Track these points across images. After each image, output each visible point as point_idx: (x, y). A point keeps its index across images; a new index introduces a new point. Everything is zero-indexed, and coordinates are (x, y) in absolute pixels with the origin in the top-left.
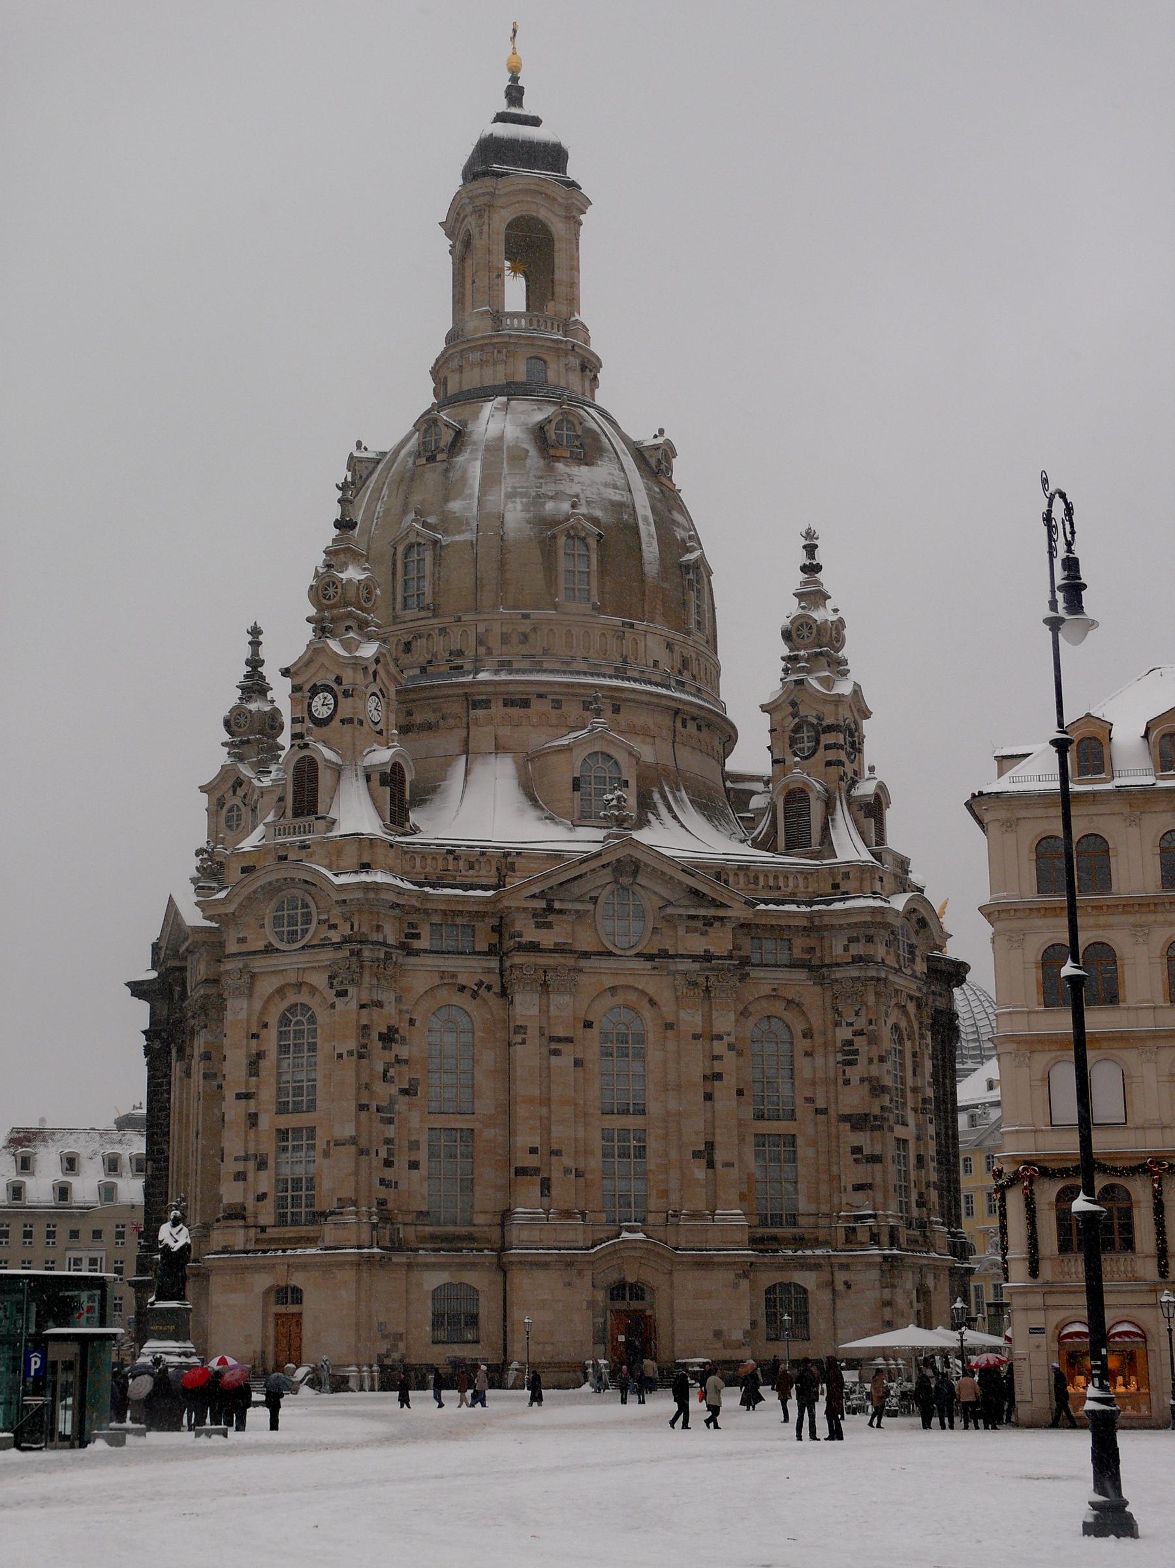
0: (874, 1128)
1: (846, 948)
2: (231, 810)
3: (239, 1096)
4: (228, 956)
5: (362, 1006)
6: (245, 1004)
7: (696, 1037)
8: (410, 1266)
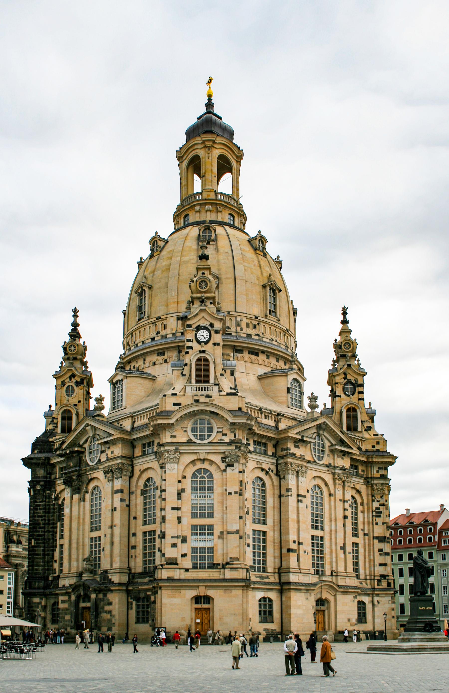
0: (388, 542)
1: (378, 472)
2: (68, 387)
3: (173, 509)
4: (168, 443)
5: (240, 472)
6: (176, 466)
7: (340, 500)
8: (253, 588)
